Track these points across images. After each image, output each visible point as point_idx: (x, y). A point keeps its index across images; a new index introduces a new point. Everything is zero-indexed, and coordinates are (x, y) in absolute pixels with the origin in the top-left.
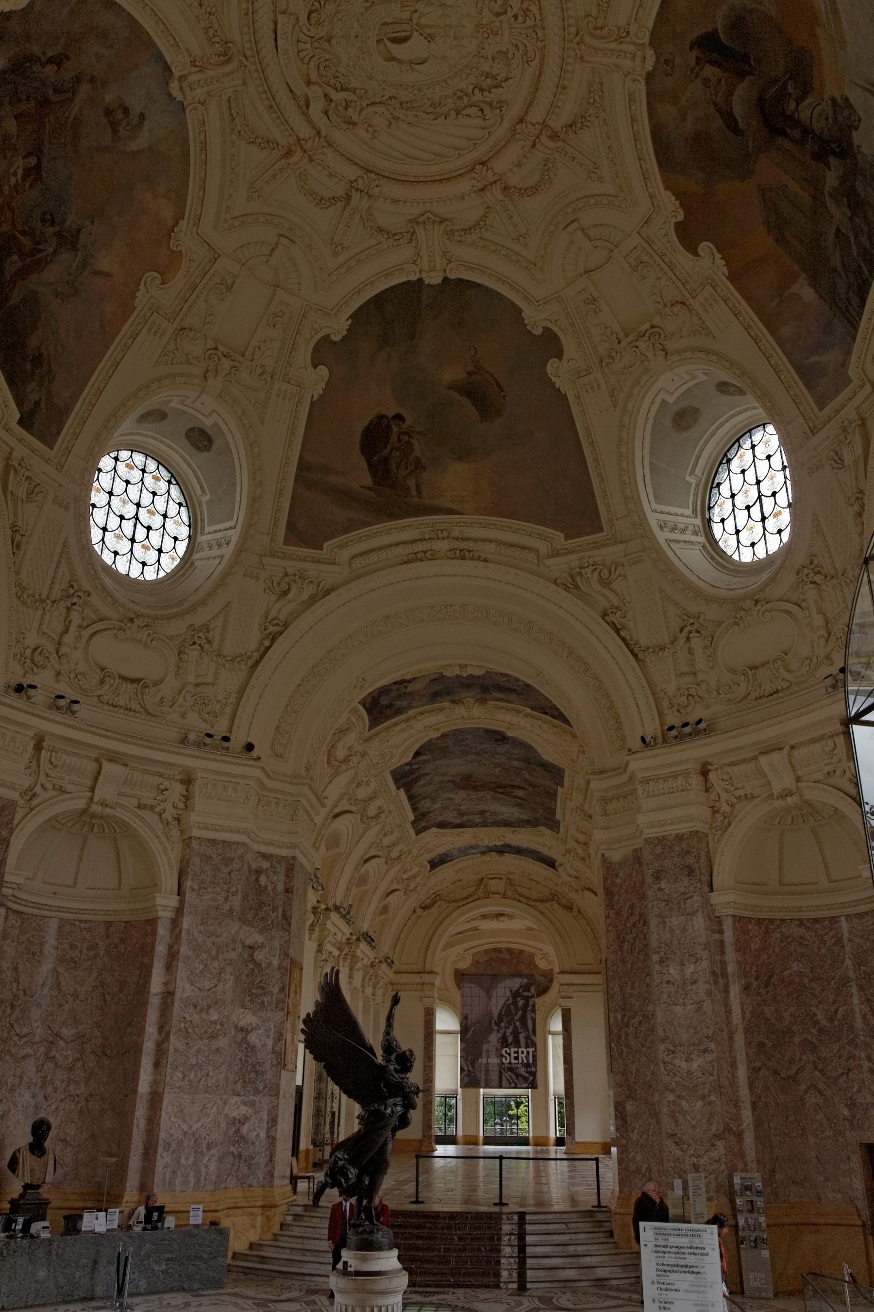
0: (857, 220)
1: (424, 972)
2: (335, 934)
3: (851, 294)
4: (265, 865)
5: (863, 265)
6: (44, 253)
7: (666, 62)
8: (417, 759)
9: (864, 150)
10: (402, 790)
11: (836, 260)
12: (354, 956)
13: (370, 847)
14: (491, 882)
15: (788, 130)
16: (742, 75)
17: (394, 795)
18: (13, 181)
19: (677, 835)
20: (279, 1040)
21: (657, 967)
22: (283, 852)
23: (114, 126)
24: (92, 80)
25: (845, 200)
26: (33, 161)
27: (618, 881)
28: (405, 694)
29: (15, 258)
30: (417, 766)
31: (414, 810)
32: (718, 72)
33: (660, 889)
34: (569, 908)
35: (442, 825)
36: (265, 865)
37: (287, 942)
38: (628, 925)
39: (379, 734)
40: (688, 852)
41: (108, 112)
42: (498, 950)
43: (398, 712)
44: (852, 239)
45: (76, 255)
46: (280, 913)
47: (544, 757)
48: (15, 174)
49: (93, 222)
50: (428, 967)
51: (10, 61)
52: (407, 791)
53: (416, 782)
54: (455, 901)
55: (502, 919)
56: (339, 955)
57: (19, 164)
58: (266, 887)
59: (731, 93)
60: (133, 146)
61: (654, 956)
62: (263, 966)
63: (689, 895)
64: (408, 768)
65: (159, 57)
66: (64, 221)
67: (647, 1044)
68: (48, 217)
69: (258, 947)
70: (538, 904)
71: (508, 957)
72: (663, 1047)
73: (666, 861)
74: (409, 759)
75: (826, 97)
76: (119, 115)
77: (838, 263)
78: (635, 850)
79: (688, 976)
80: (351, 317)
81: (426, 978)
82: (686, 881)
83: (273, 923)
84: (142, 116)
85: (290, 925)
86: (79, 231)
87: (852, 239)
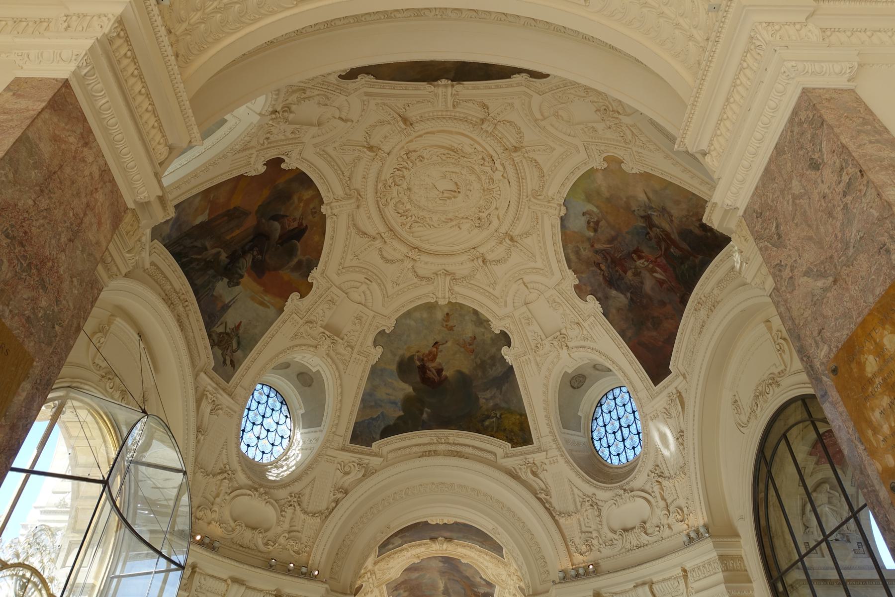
0: (203, 263)
3: (182, 247)
5: (188, 259)
6: (662, 233)
7: (315, 212)
9: (220, 282)
11: (198, 244)
15: (252, 243)
16: (280, 237)
18: (646, 263)
23: (597, 223)
24: (592, 246)
25: (212, 260)
26: (634, 256)
29: (672, 250)
32: (292, 228)
41: (595, 230)
44: (199, 257)
45: (651, 214)
48: (643, 263)
49: (634, 211)
51: (611, 288)
57: (640, 263)
59: (282, 228)
60: (595, 209)
65: (563, 226)
66: (644, 227)
68: (648, 237)
75: (246, 275)
76: (592, 224)
77: (195, 244)
80: (510, 78)
84: (584, 214)
86: (642, 217)
87: (199, 257)
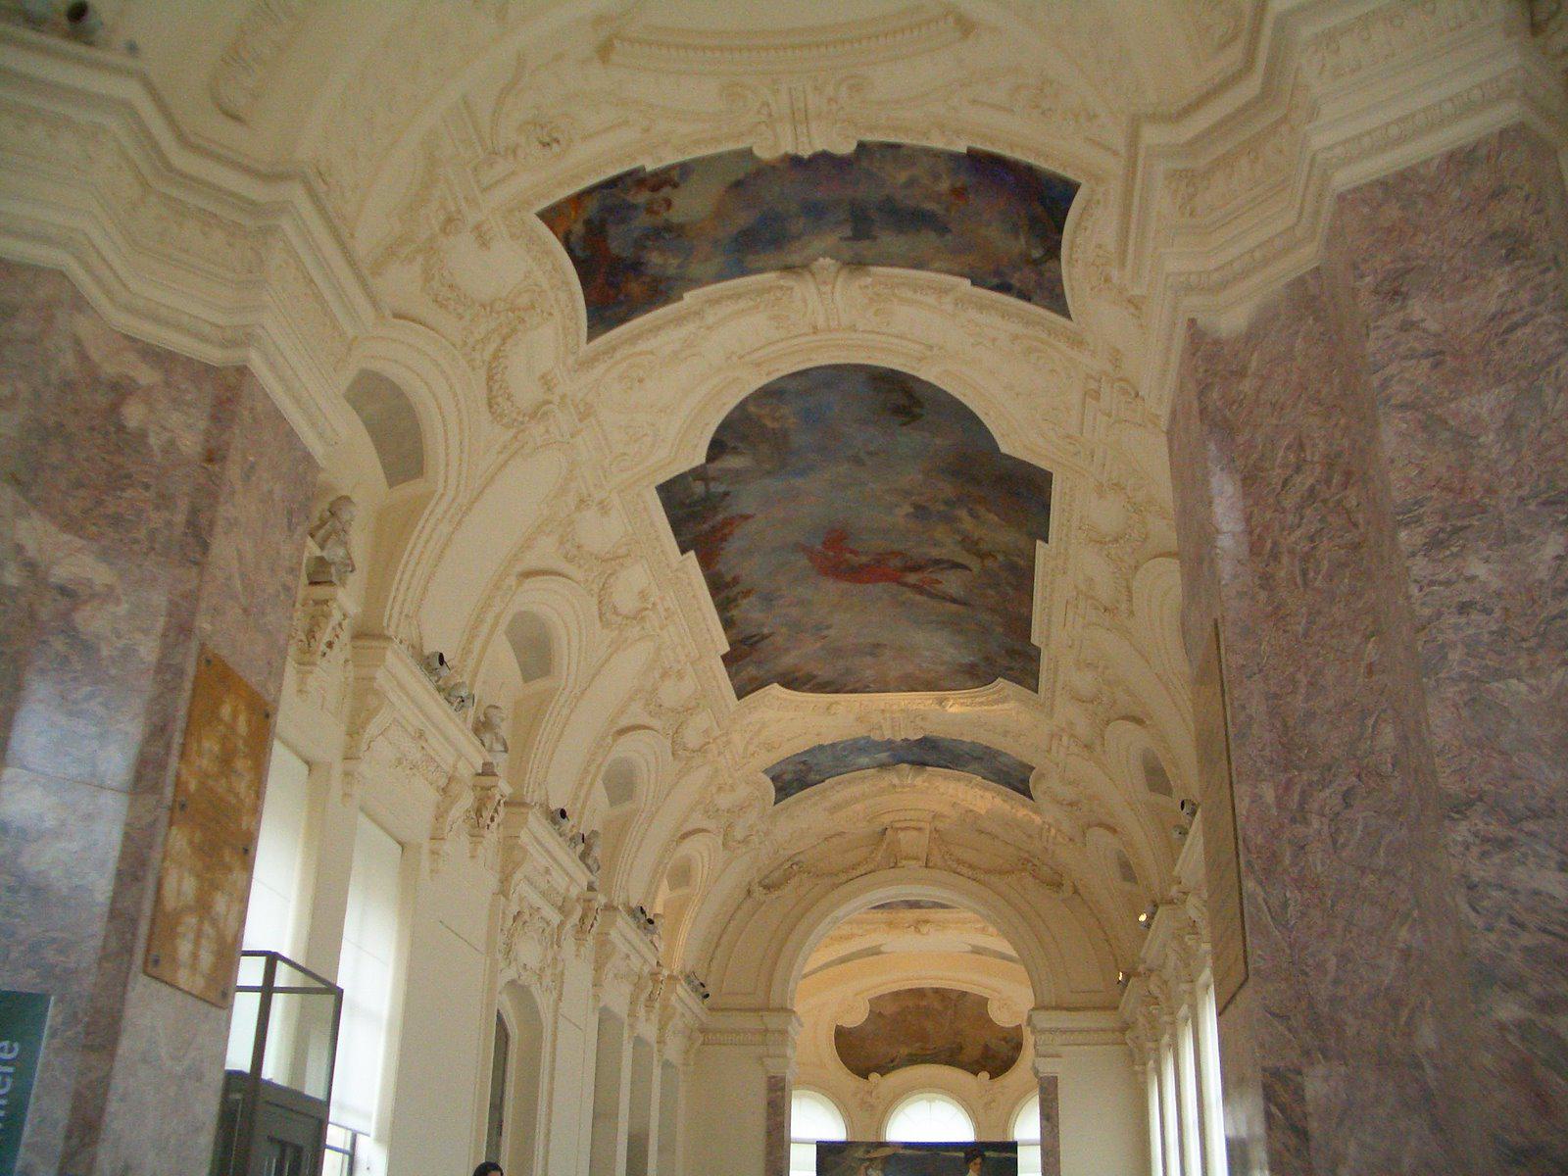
1: (768, 1009)
2: (547, 871)
4: (146, 375)
8: (719, 464)
10: (692, 554)
12: (603, 941)
13: (631, 699)
14: (901, 835)
17: (675, 565)
19: (1451, 156)
20: (136, 879)
21: (1420, 567)
22: (214, 355)
27: (1247, 386)
28: (669, 227)
30: (722, 489)
31: (728, 624)
33: (1407, 326)
34: (1058, 886)
35: (791, 682)
36: (146, 375)
37: (193, 597)
38: (1289, 502)
39: (614, 349)
40: (1497, 194)
42: (919, 993)
43: (660, 292)
46: (180, 518)
47: (1004, 449)
50: (775, 1002)
52: (706, 561)
53: (724, 539)
54: (832, 874)
55: (924, 929)
56: (562, 924)
58: (142, 435)
61: (1403, 535)
62: (105, 652)
63: (1517, 318)
64: (699, 488)
67: (1380, 861)
69: (93, 596)
70: (994, 879)
71: (937, 1005)
72: (1462, 831)
73: (1421, 238)
74: (700, 458)
78: (1301, 281)
79: (1543, 573)
81: (773, 1021)
82: (1501, 281)
83: (152, 535)
85: (205, 547)
